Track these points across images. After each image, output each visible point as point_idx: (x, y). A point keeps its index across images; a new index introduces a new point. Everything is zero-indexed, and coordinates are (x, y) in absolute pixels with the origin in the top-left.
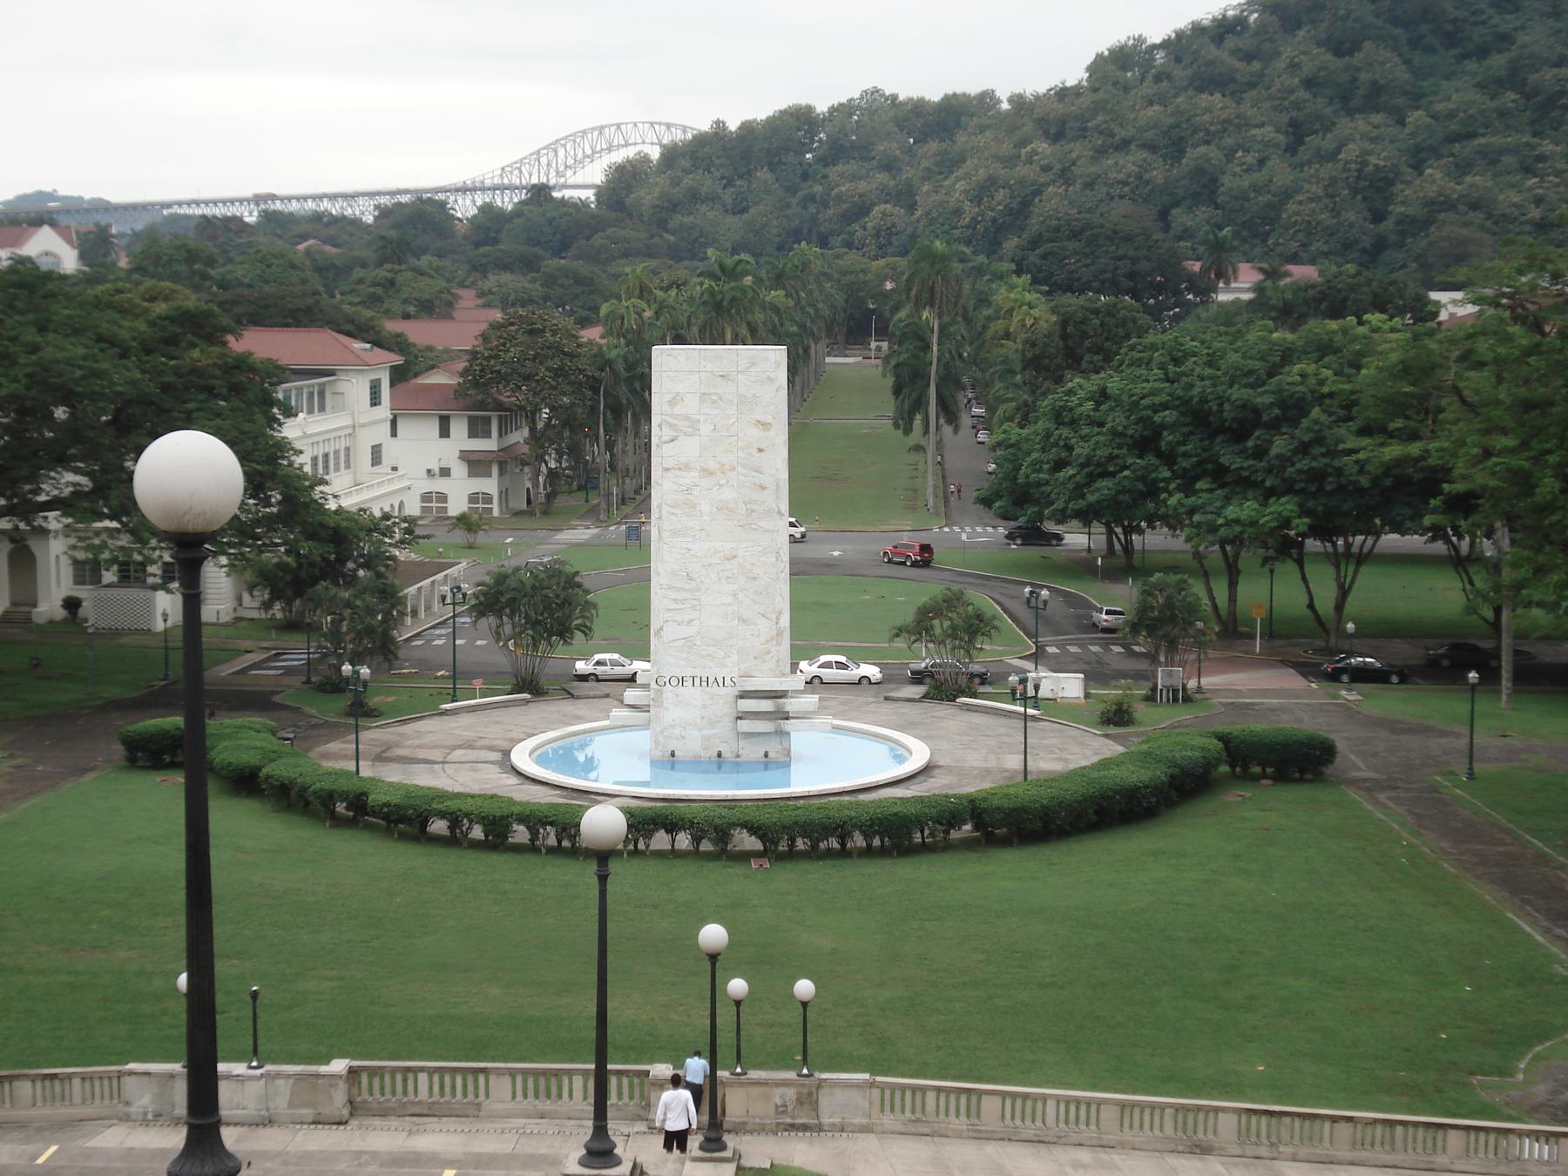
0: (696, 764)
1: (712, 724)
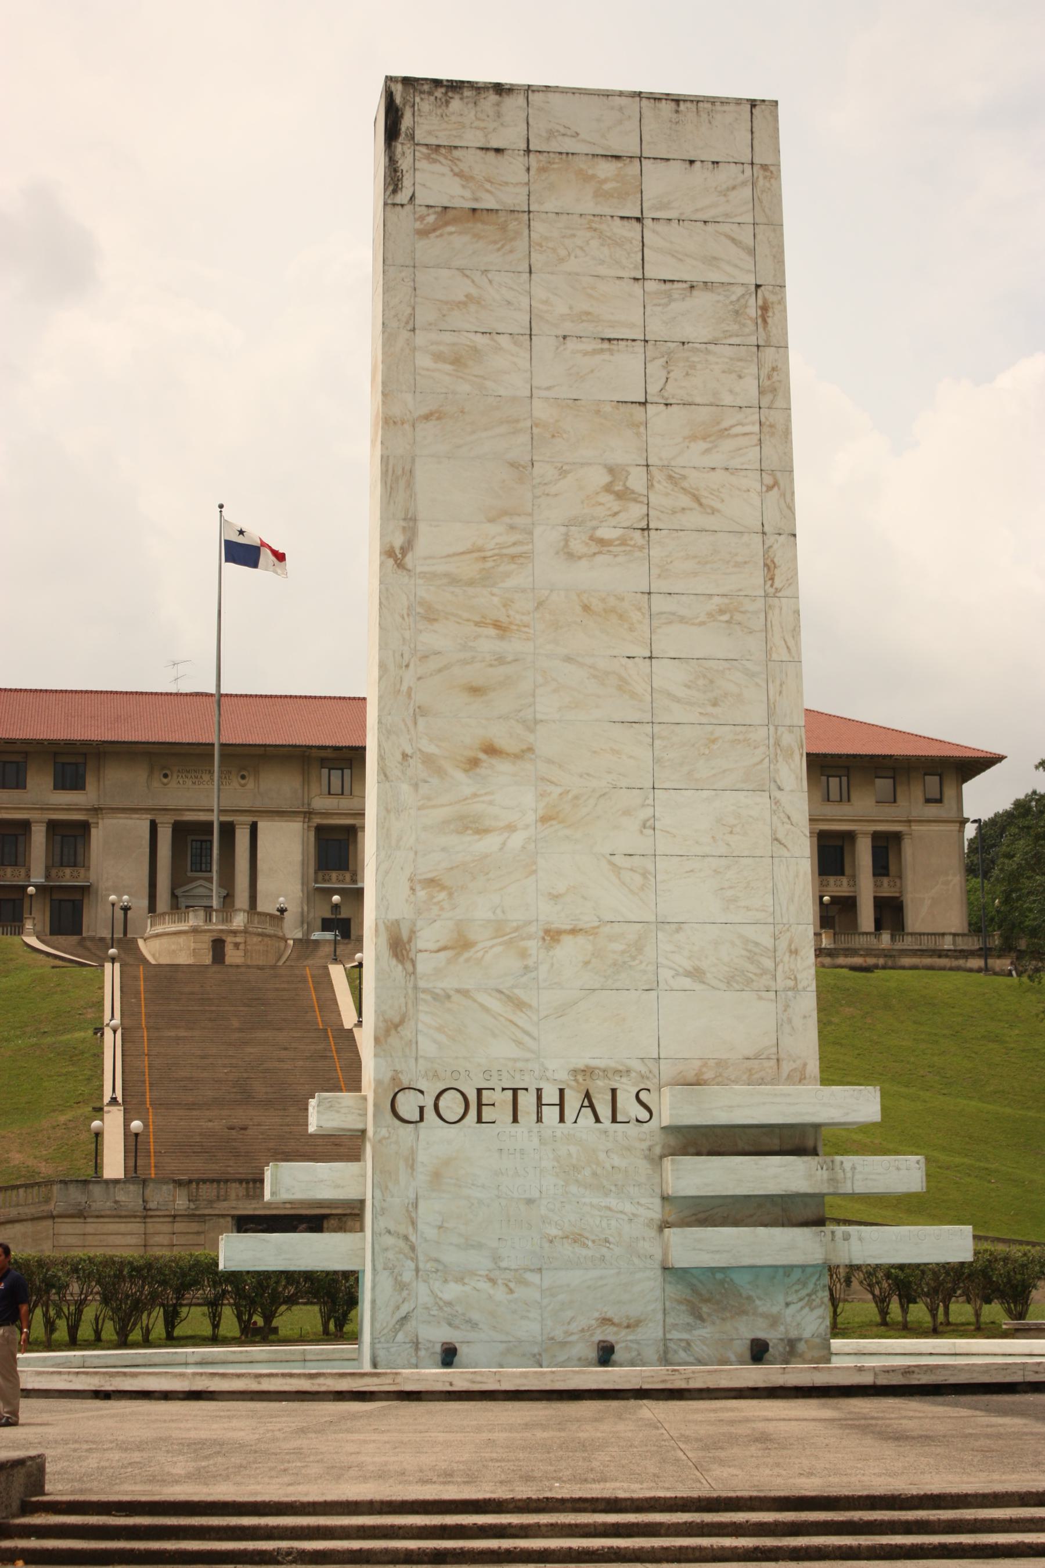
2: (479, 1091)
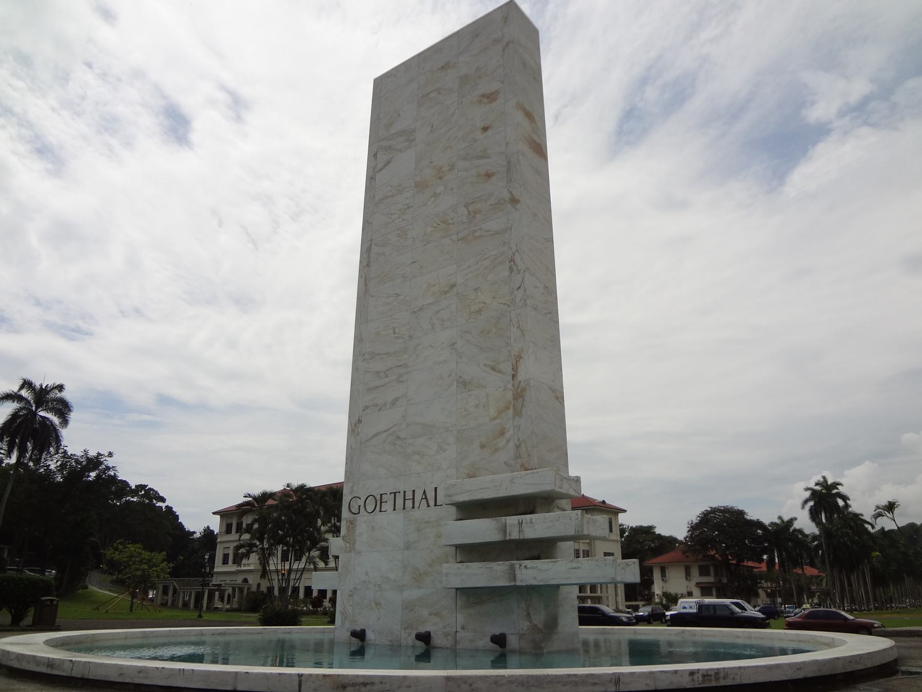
0: (393, 652)
1: (418, 578)
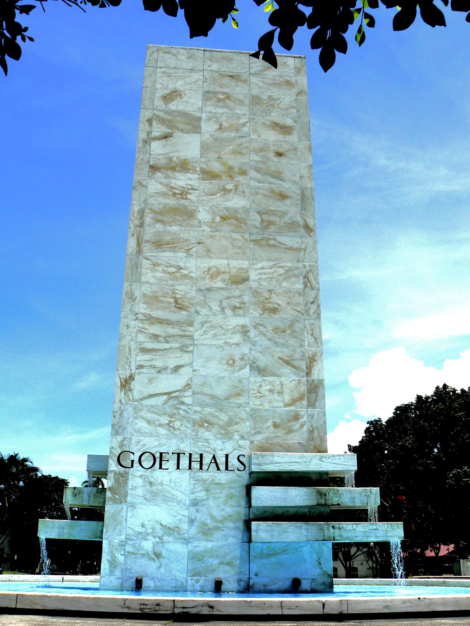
1: (206, 532)
2: (161, 454)
